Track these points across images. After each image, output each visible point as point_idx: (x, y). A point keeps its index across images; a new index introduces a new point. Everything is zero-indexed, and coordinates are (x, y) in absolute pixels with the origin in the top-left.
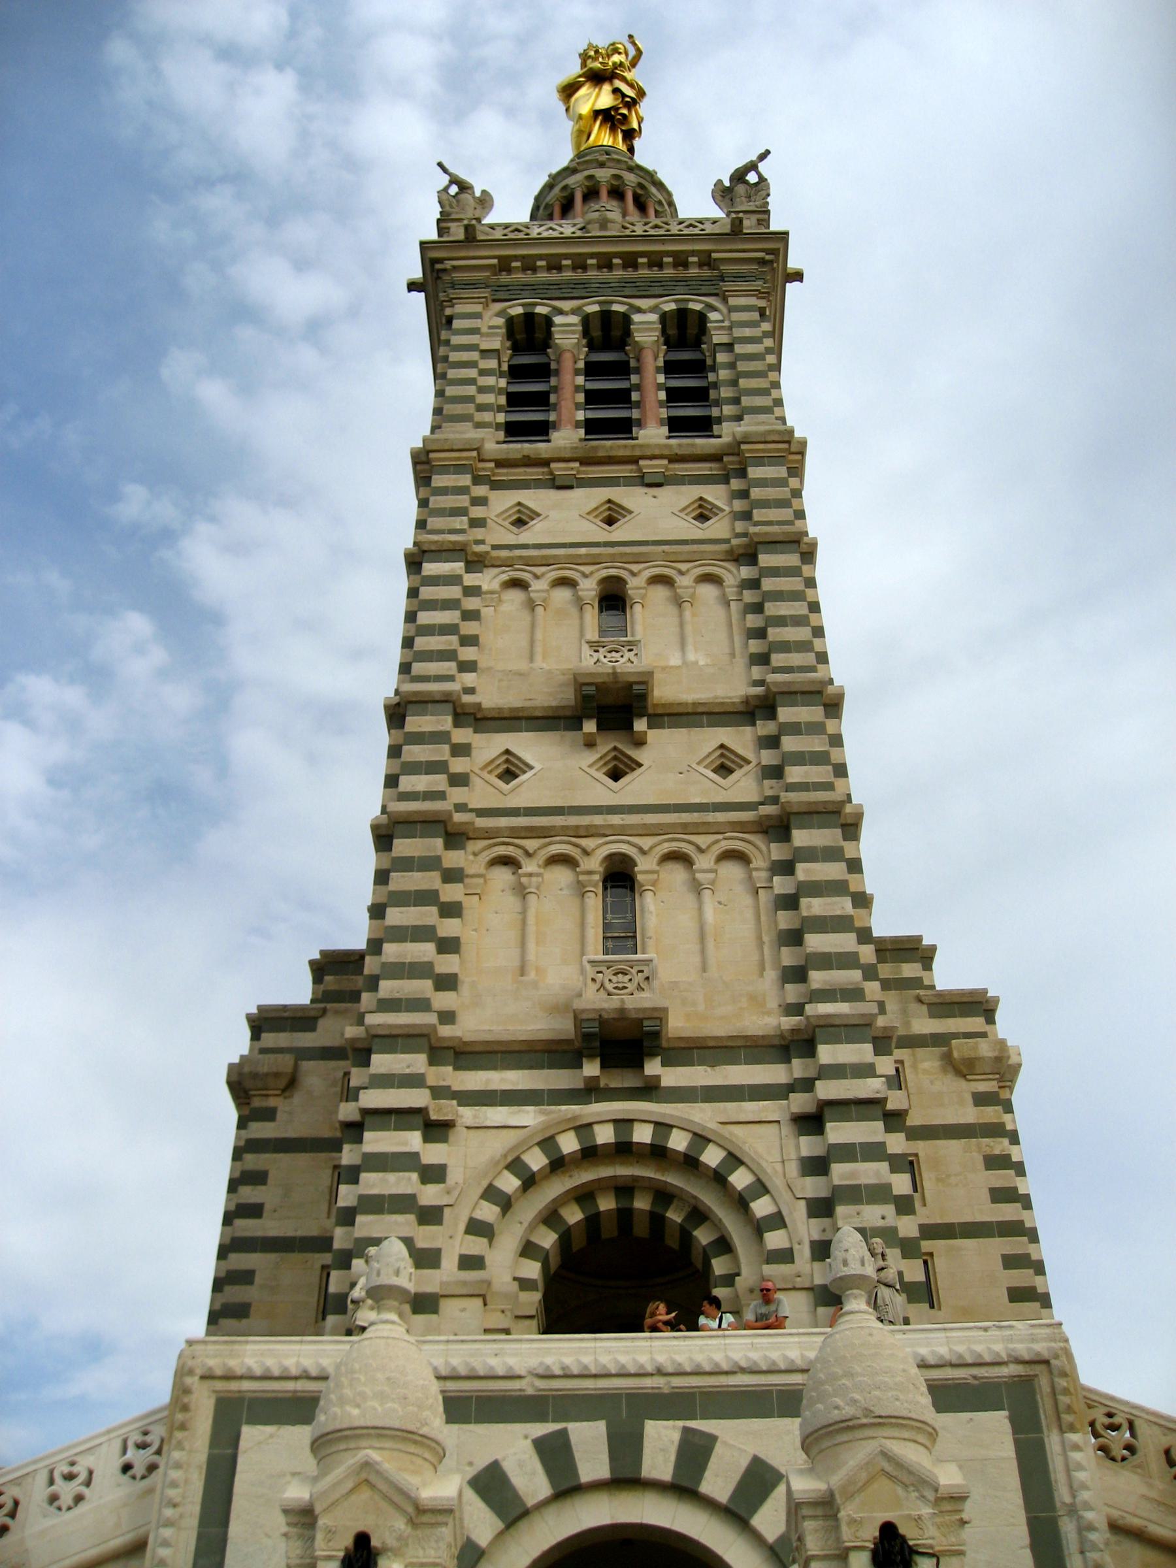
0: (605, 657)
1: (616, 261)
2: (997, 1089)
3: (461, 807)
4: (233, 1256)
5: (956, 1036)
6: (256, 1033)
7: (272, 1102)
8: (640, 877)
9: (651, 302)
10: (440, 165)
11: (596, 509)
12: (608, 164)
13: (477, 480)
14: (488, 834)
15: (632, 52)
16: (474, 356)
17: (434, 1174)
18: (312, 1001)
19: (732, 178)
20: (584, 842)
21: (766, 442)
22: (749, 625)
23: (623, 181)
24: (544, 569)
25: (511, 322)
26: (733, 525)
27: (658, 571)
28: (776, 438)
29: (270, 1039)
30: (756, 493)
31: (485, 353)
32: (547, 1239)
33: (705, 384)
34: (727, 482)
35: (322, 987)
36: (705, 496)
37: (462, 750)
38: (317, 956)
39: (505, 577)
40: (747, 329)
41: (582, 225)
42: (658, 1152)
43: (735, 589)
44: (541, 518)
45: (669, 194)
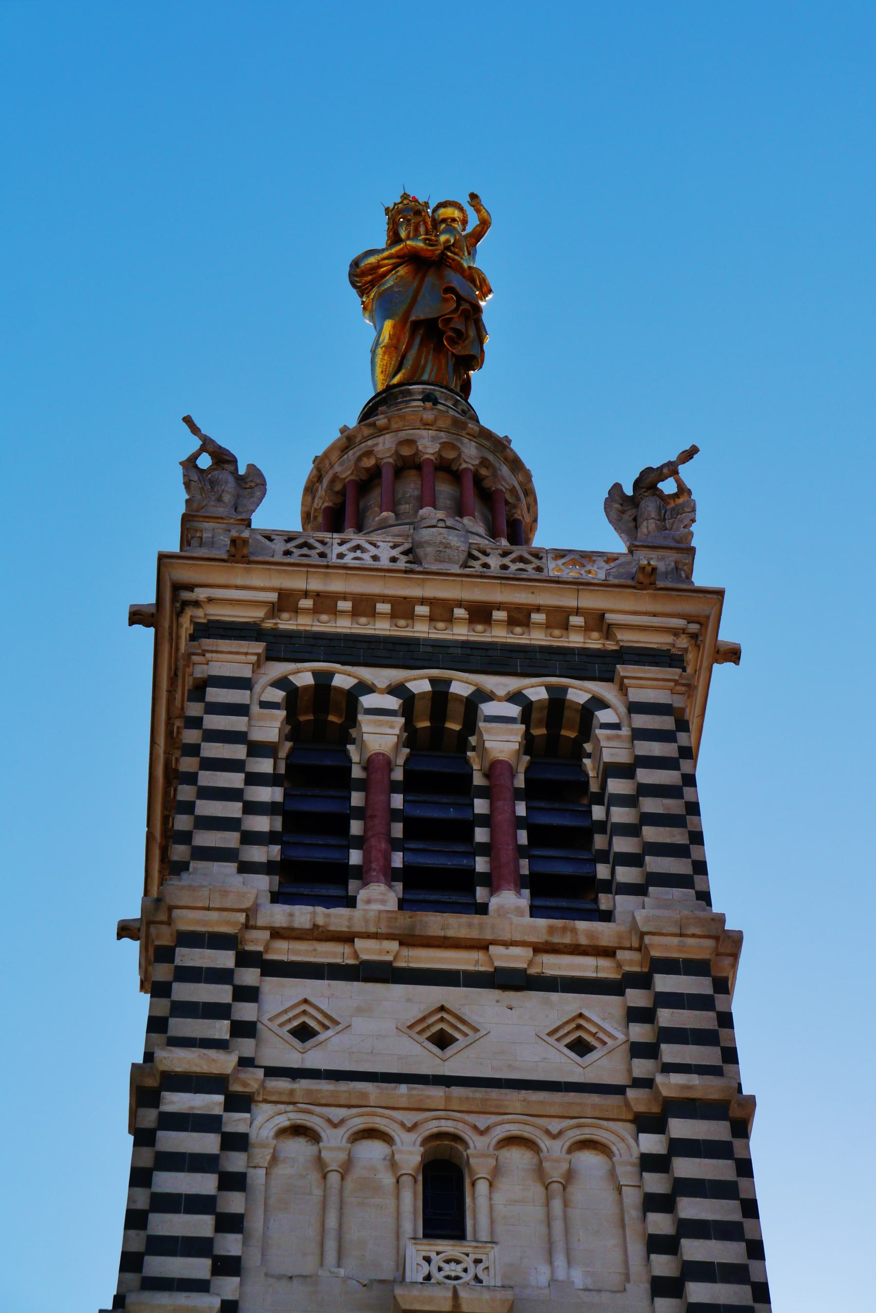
0: (440, 1269)
1: (460, 612)
9: (511, 684)
10: (188, 420)
11: (423, 1019)
13: (245, 959)
15: (473, 221)
16: (239, 752)
19: (637, 484)
22: (652, 1230)
23: (459, 455)
24: (342, 1113)
26: (630, 1064)
27: (514, 1130)
30: (666, 1017)
31: (257, 749)
33: (584, 824)
34: (622, 993)
36: (586, 1013)
39: (283, 1121)
41: (407, 546)
43: (629, 1168)
44: (339, 1028)
45: (528, 476)
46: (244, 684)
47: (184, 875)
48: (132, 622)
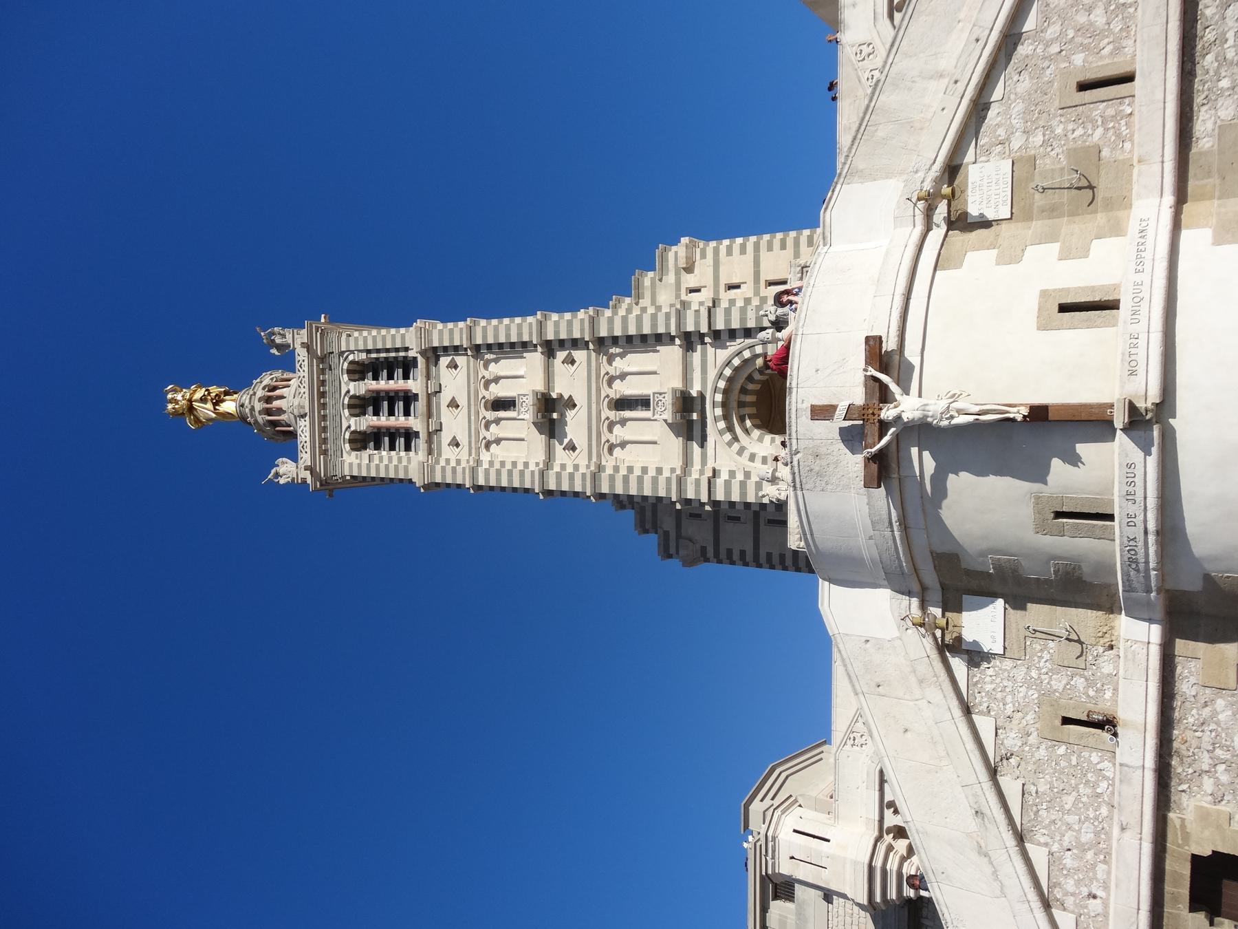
2: (699, 249)
3: (588, 467)
4: (761, 561)
5: (676, 264)
6: (670, 556)
7: (698, 546)
8: (618, 397)
12: (252, 404)
14: (599, 456)
17: (732, 474)
18: (656, 533)
20: (603, 419)
21: (421, 338)
25: (353, 449)
28: (419, 333)
29: (672, 551)
32: (756, 433)
35: (651, 530)
37: (563, 467)
38: (637, 532)
39: (484, 451)
40: (359, 343)
42: (726, 392)
46: (351, 465)
47: (413, 480)
48: (333, 496)
